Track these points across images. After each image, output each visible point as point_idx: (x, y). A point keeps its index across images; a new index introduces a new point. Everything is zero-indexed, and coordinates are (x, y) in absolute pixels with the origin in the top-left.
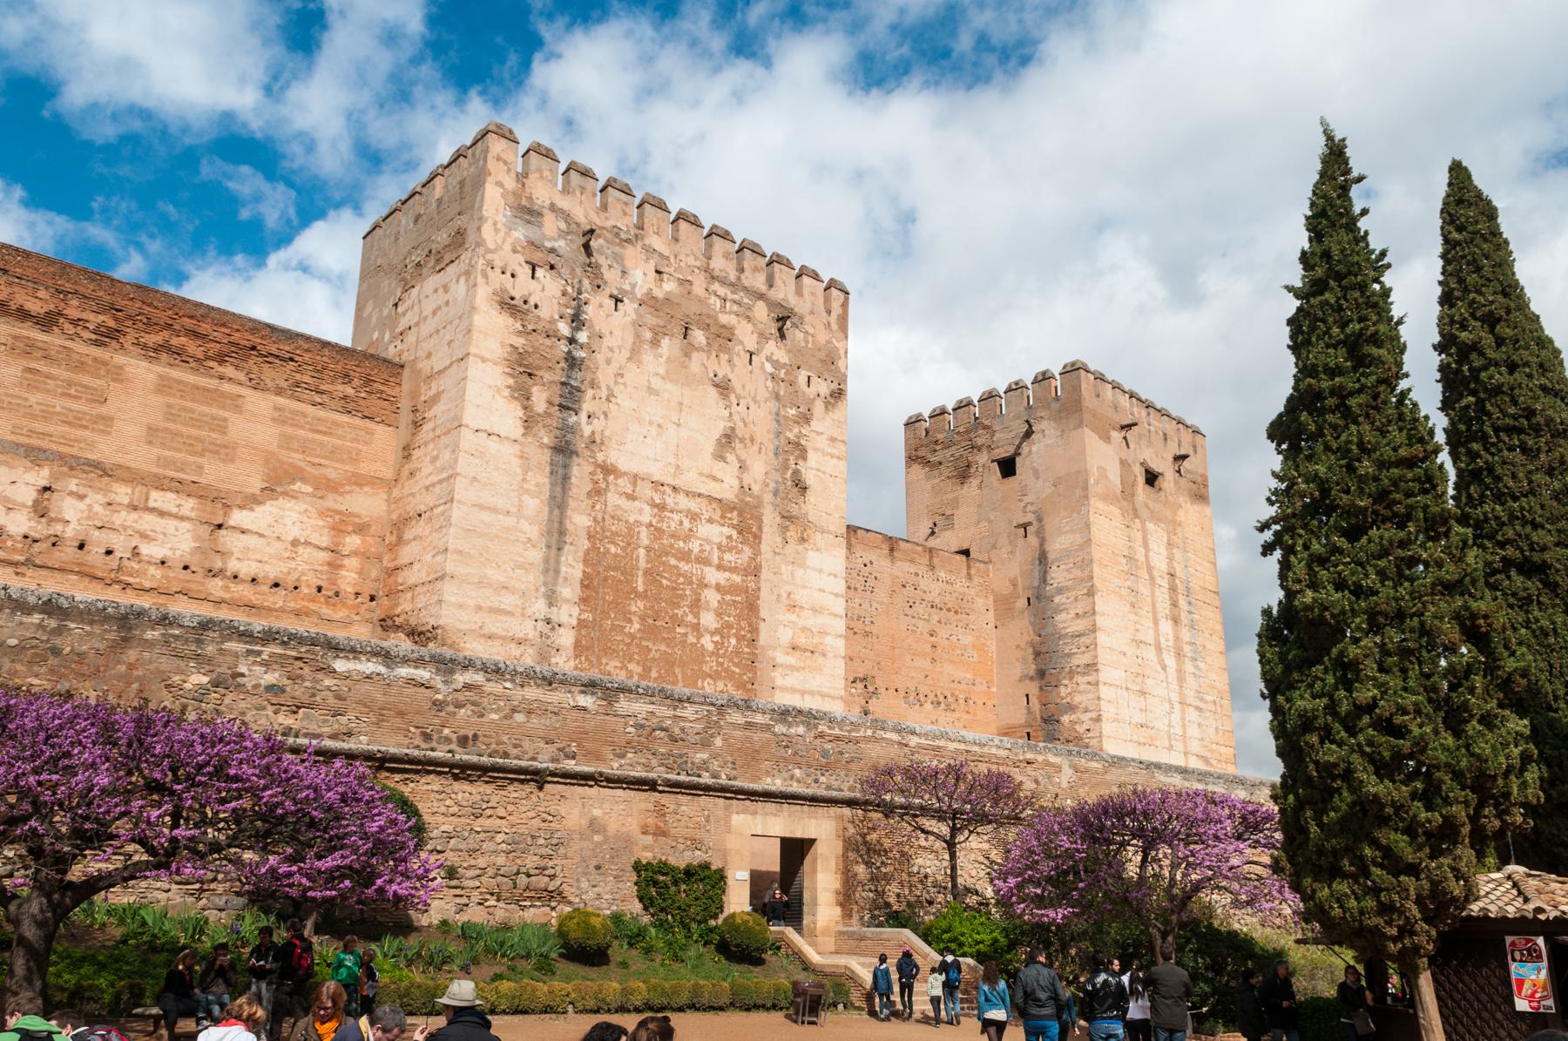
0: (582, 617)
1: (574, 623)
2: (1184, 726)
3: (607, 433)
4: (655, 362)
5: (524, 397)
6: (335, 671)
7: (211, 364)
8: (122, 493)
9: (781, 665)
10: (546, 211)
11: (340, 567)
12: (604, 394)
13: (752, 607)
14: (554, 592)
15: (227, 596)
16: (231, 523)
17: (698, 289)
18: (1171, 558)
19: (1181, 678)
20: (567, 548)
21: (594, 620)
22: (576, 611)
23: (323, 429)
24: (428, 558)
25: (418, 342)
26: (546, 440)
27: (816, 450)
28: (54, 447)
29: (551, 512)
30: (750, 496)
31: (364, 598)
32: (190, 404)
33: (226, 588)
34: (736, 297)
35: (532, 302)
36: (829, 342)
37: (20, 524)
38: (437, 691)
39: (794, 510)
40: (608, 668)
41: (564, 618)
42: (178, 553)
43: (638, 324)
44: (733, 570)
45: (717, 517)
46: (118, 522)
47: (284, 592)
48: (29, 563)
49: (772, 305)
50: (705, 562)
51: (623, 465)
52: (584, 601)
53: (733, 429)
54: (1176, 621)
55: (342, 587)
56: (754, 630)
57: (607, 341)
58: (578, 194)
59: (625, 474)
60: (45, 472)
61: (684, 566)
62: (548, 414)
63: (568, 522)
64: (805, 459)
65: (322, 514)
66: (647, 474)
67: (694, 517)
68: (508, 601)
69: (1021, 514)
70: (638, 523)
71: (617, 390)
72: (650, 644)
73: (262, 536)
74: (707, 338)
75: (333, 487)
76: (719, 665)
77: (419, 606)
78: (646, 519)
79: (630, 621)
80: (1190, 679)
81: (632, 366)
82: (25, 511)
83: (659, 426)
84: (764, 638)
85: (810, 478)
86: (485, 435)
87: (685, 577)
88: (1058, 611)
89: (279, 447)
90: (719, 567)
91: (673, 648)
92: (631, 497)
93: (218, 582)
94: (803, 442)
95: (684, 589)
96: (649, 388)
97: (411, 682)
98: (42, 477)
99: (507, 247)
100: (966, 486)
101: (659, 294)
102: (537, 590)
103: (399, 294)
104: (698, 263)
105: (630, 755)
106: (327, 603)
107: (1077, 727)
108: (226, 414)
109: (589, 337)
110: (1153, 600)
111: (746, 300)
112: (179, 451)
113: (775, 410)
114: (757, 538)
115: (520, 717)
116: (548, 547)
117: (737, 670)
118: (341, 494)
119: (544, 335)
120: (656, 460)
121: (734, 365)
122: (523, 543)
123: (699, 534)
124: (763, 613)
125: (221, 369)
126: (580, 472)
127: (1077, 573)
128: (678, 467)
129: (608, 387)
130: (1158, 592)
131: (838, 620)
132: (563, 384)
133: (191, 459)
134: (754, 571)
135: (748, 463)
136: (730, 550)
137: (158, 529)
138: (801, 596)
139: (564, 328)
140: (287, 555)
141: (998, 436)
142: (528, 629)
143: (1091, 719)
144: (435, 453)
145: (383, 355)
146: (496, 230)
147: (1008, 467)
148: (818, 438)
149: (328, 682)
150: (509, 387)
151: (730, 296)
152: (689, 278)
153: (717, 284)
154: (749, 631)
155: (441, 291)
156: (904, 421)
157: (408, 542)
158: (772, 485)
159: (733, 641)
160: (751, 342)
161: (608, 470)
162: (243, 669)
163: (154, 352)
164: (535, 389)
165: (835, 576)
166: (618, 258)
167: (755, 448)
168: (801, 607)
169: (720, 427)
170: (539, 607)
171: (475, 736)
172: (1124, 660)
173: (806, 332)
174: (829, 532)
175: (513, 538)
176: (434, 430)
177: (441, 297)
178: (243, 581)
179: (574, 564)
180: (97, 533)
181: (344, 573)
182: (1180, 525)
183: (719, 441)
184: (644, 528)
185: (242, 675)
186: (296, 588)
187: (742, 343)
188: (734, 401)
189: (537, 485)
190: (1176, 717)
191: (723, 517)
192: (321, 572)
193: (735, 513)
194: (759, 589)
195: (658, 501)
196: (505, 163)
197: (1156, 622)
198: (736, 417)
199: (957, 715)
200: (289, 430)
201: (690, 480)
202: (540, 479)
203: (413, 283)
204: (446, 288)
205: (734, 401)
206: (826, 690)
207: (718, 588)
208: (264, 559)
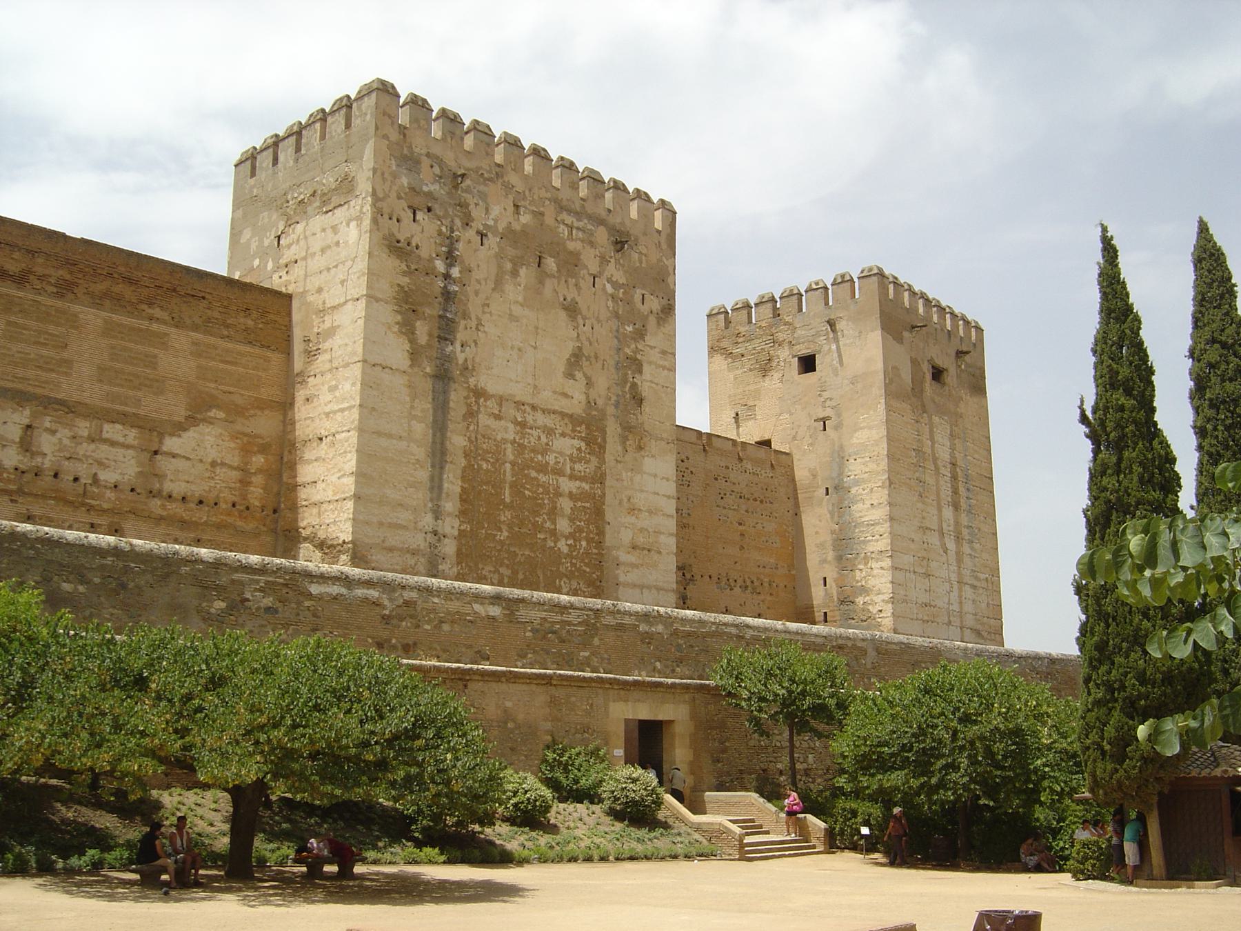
0: (462, 528)
1: (456, 533)
2: (961, 603)
3: (477, 360)
4: (514, 292)
5: (407, 330)
6: (311, 595)
7: (144, 307)
8: (84, 427)
9: (623, 564)
10: (424, 158)
11: (249, 483)
12: (474, 323)
13: (598, 512)
14: (439, 506)
15: (164, 513)
16: (165, 449)
17: (549, 220)
18: (953, 449)
19: (959, 561)
20: (447, 466)
21: (471, 530)
22: (457, 523)
23: (229, 359)
24: (334, 478)
25: (306, 276)
26: (428, 370)
27: (650, 363)
28: (31, 389)
29: (434, 435)
30: (596, 409)
31: (269, 511)
32: (128, 344)
33: (163, 507)
34: (581, 224)
35: (414, 244)
36: (660, 260)
37: (12, 458)
38: (384, 607)
39: (632, 420)
40: (484, 573)
41: (448, 530)
42: (126, 477)
43: (499, 256)
44: (581, 479)
45: (568, 431)
46: (81, 453)
47: (207, 509)
48: (20, 491)
49: (612, 230)
50: (559, 472)
51: (492, 387)
52: (463, 513)
53: (580, 349)
54: (956, 506)
55: (251, 501)
56: (601, 533)
57: (477, 275)
58: (449, 139)
59: (493, 396)
60: (27, 412)
61: (543, 478)
62: (429, 346)
63: (448, 442)
64: (641, 372)
65: (234, 437)
66: (510, 395)
67: (550, 432)
68: (404, 517)
69: (820, 409)
70: (504, 441)
71: (485, 318)
72: (517, 550)
73: (188, 459)
74: (558, 265)
75: (235, 412)
76: (573, 565)
77: (327, 522)
78: (511, 436)
79: (500, 530)
80: (967, 560)
81: (496, 295)
82: (15, 447)
83: (520, 350)
84: (609, 540)
85: (645, 389)
86: (381, 369)
87: (543, 486)
88: (854, 502)
89: (197, 378)
90: (572, 477)
91: (534, 552)
92: (498, 417)
93: (156, 503)
94: (639, 357)
95: (543, 499)
96: (511, 315)
97: (365, 600)
98: (22, 417)
99: (393, 195)
100: (767, 378)
101: (516, 226)
102: (425, 505)
103: (281, 228)
104: (549, 195)
105: (530, 656)
106: (240, 516)
107: (870, 608)
108: (156, 351)
109: (460, 272)
110: (937, 488)
111: (589, 227)
112: (122, 386)
113: (615, 328)
114: (602, 447)
115: (446, 627)
116: (433, 466)
117: (588, 570)
118: (247, 418)
119: (424, 273)
120: (517, 382)
121: (580, 288)
122: (413, 464)
123: (554, 448)
124: (609, 516)
125: (151, 311)
126: (457, 397)
127: (872, 466)
128: (535, 387)
129: (478, 319)
130: (942, 483)
131: (671, 519)
132: (440, 317)
133: (131, 393)
134: (599, 478)
135: (594, 379)
136: (580, 460)
137: (110, 457)
138: (640, 500)
139: (440, 266)
140: (207, 475)
141: (799, 332)
142: (419, 541)
143: (883, 601)
144: (334, 383)
145: (266, 285)
146: (384, 180)
147: (808, 364)
148: (652, 352)
149: (307, 604)
150: (397, 323)
151: (576, 224)
152: (542, 209)
153: (565, 213)
154: (597, 534)
155: (329, 231)
156: (707, 312)
157: (309, 462)
158: (614, 398)
159: (584, 543)
160: (594, 267)
161: (479, 393)
162: (248, 595)
163: (98, 301)
164: (418, 324)
165: (668, 480)
166: (483, 196)
167: (599, 365)
168: (640, 510)
169: (570, 347)
170: (428, 520)
171: (415, 644)
172: (912, 546)
173: (640, 253)
174: (662, 439)
175: (406, 460)
176: (331, 361)
177: (330, 237)
178: (176, 500)
179: (454, 481)
180: (67, 463)
181: (252, 488)
182: (961, 417)
183: (568, 360)
184: (509, 445)
185: (248, 600)
186: (216, 504)
187: (586, 267)
188: (581, 322)
189: (423, 411)
190: (955, 594)
191: (573, 431)
192: (234, 489)
193: (584, 427)
194: (604, 494)
195: (519, 420)
196: (390, 116)
197: (940, 509)
198: (583, 338)
199: (761, 597)
200: (204, 362)
201: (546, 397)
202: (425, 406)
203: (297, 219)
204: (334, 229)
205: (581, 322)
206: (661, 584)
207: (571, 495)
208: (190, 480)
